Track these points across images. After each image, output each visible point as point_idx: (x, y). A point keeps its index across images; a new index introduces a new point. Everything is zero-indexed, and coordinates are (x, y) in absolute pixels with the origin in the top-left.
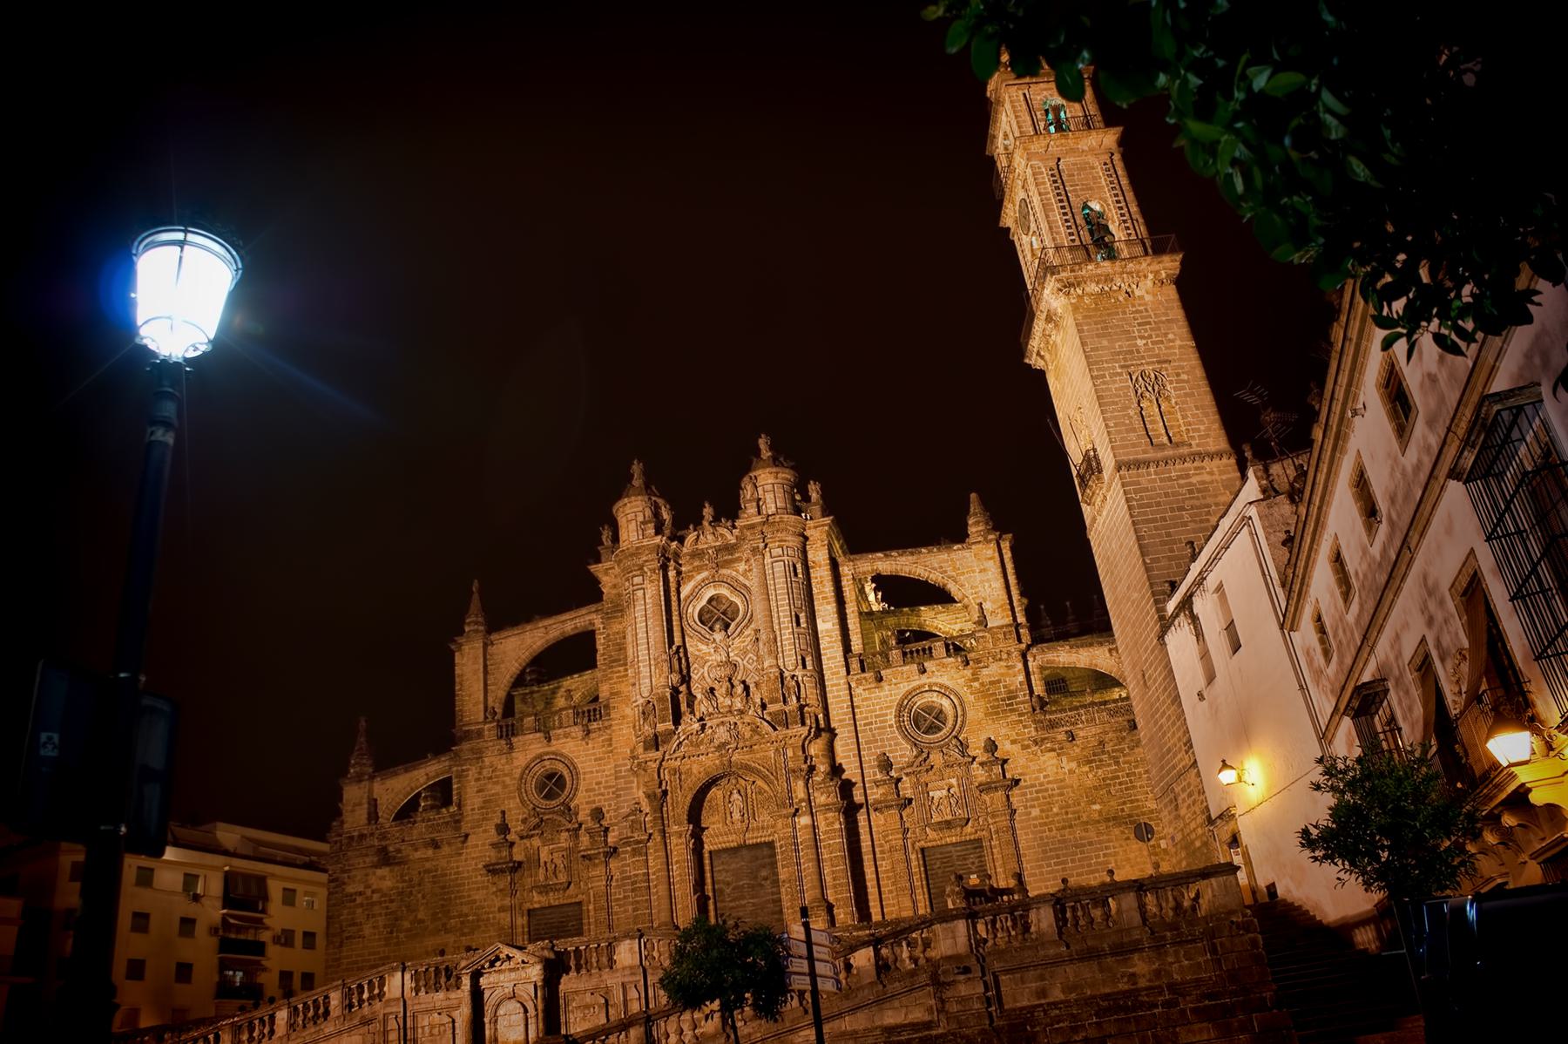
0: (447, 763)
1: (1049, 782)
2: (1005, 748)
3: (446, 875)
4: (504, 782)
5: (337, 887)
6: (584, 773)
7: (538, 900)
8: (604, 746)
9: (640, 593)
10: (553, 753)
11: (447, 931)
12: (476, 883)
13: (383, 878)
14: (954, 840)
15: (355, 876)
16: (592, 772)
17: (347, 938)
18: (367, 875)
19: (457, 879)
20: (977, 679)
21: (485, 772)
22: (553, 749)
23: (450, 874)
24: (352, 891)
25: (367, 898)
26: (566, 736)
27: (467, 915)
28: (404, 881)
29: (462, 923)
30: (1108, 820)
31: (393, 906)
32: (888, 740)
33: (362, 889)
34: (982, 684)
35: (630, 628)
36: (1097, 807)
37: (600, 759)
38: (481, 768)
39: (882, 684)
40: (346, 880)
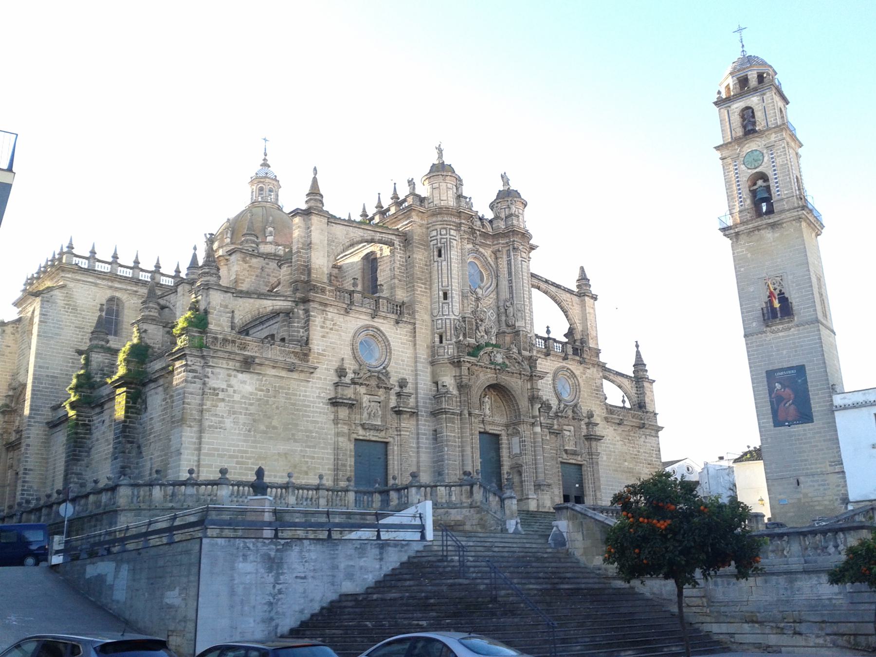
0: (290, 303)
1: (610, 444)
2: (597, 419)
3: (295, 395)
4: (341, 336)
5: (195, 377)
6: (394, 350)
7: (361, 434)
8: (407, 335)
9: (455, 242)
10: (376, 328)
11: (295, 441)
12: (318, 407)
13: (244, 382)
14: (574, 462)
15: (219, 374)
16: (399, 351)
17: (210, 427)
18: (229, 375)
19: (304, 401)
20: (585, 374)
21: (328, 322)
22: (375, 324)
23: (300, 396)
24: (216, 386)
25: (229, 396)
26: (385, 318)
27: (311, 432)
28: (262, 390)
29: (307, 436)
30: (630, 472)
31: (253, 409)
32: (549, 392)
33: (224, 387)
34: (586, 377)
35: (444, 263)
36: (626, 464)
37: (404, 344)
38: (325, 319)
39: (548, 358)
40: (210, 375)
